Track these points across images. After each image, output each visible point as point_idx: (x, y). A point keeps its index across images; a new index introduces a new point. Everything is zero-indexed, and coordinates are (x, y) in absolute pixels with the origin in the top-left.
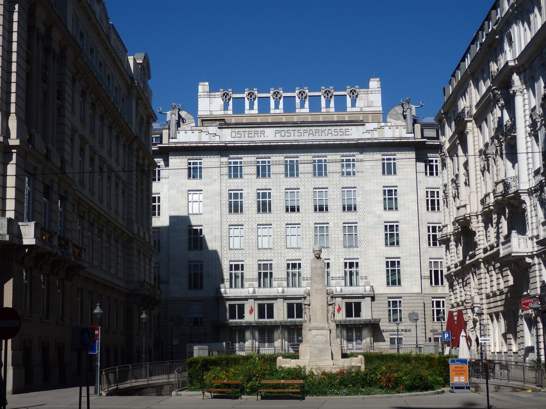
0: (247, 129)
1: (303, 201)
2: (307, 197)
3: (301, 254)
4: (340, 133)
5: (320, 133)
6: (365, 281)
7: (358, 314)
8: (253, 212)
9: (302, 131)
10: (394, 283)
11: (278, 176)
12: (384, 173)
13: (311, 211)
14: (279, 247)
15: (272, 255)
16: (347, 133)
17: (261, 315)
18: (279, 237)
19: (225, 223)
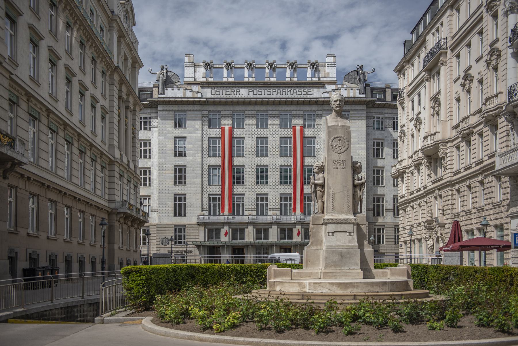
4: (303, 93)
5: (287, 93)
11: (250, 127)
13: (277, 156)
14: (250, 184)
15: (245, 190)
16: (309, 93)
18: (250, 176)
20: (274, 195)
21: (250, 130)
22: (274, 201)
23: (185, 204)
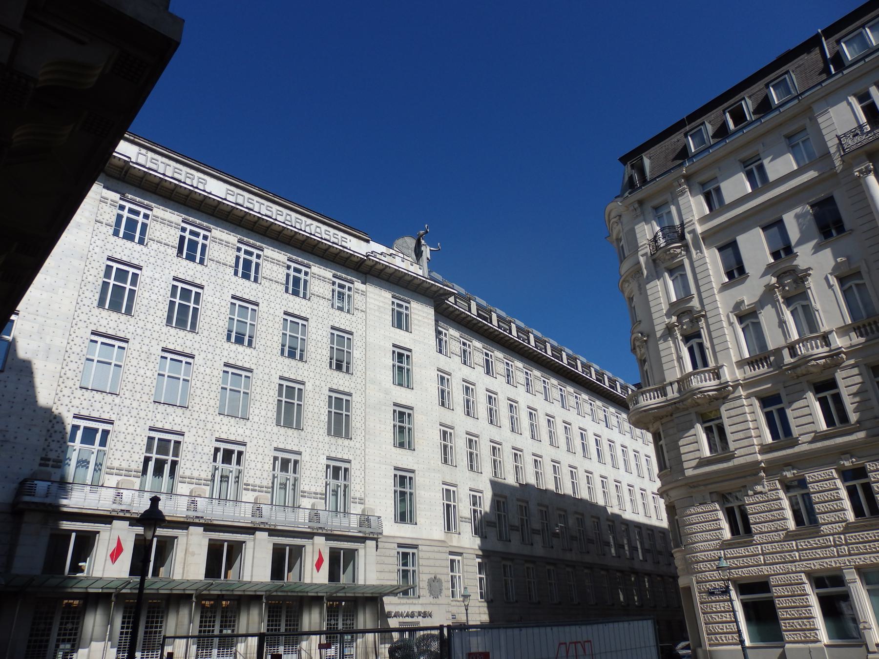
1: (264, 329)
8: (158, 321)
14: (203, 409)
15: (186, 422)
20: (260, 450)
22: (259, 466)
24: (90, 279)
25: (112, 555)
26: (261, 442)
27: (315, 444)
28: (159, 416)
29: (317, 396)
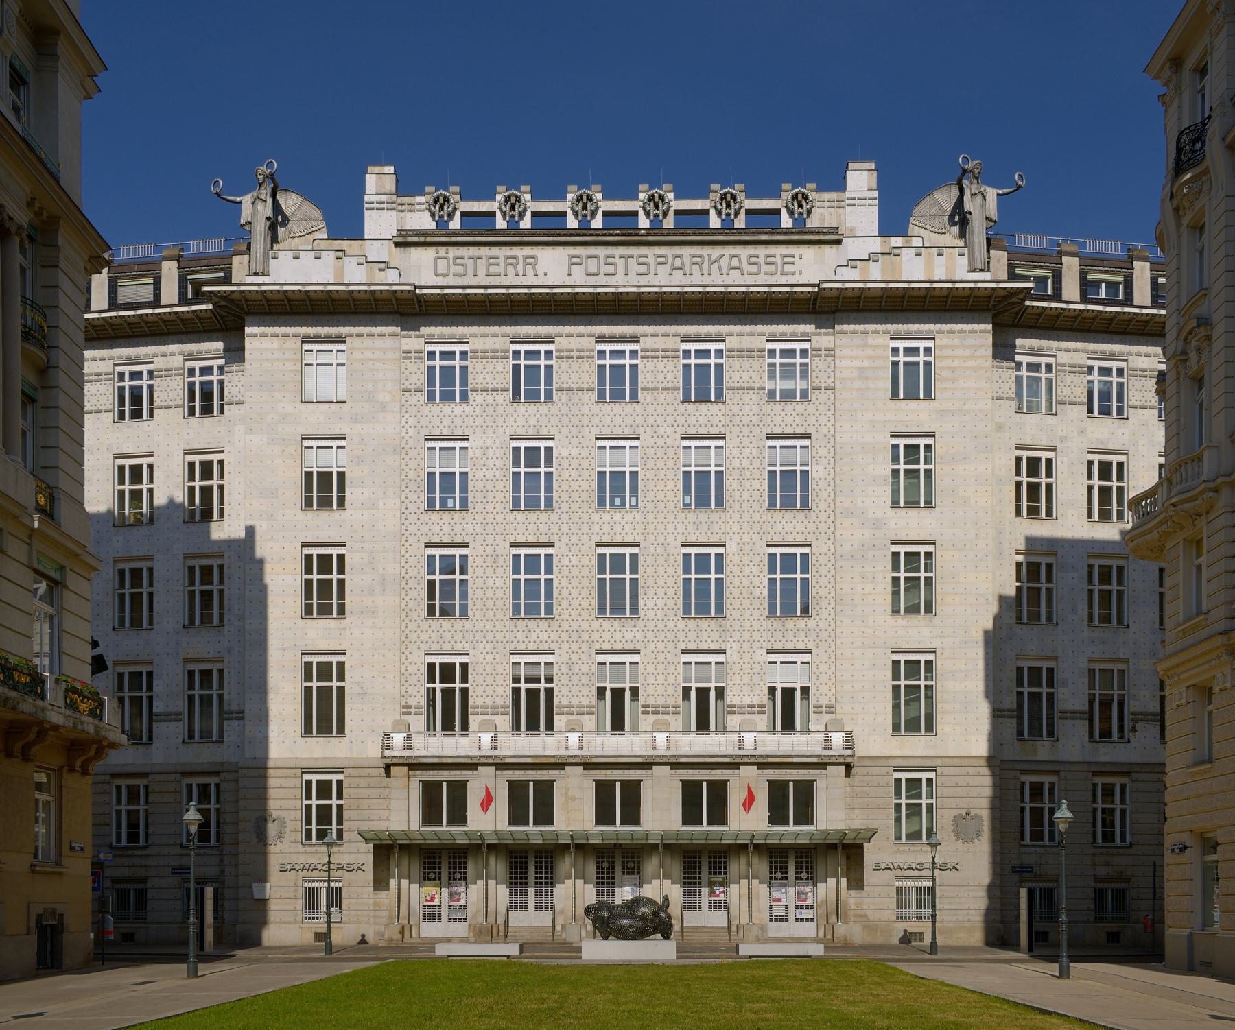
0: (485, 251)
2: (660, 464)
3: (639, 636)
4: (765, 268)
5: (705, 266)
6: (826, 718)
7: (805, 816)
8: (499, 507)
9: (651, 260)
10: (913, 726)
11: (575, 398)
12: (895, 395)
13: (671, 506)
14: (574, 614)
15: (554, 636)
16: (787, 268)
17: (517, 816)
18: (575, 583)
19: (412, 539)
20: (661, 657)
21: (575, 410)
22: (661, 679)
23: (341, 691)
24: (411, 475)
25: (482, 805)
26: (660, 646)
27: (746, 635)
28: (520, 636)
29: (746, 560)
